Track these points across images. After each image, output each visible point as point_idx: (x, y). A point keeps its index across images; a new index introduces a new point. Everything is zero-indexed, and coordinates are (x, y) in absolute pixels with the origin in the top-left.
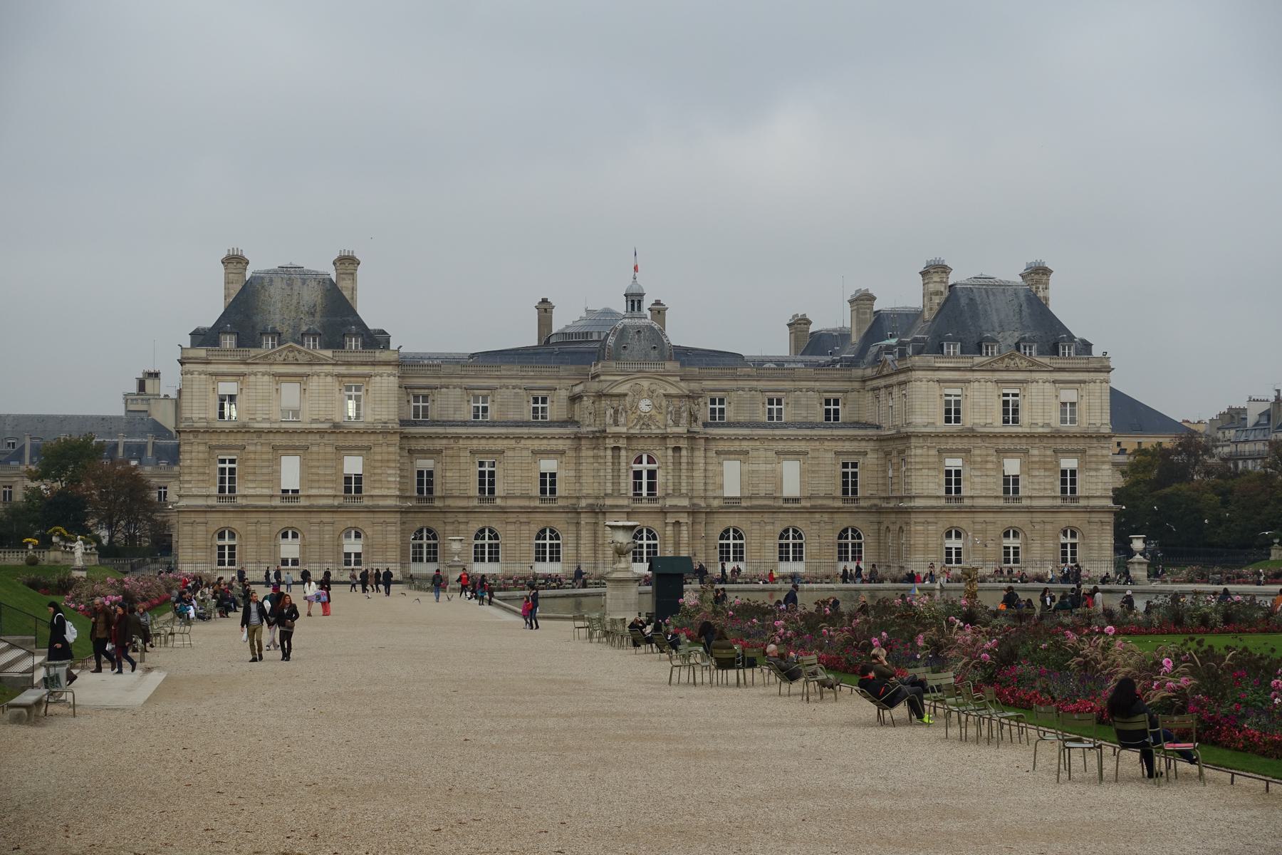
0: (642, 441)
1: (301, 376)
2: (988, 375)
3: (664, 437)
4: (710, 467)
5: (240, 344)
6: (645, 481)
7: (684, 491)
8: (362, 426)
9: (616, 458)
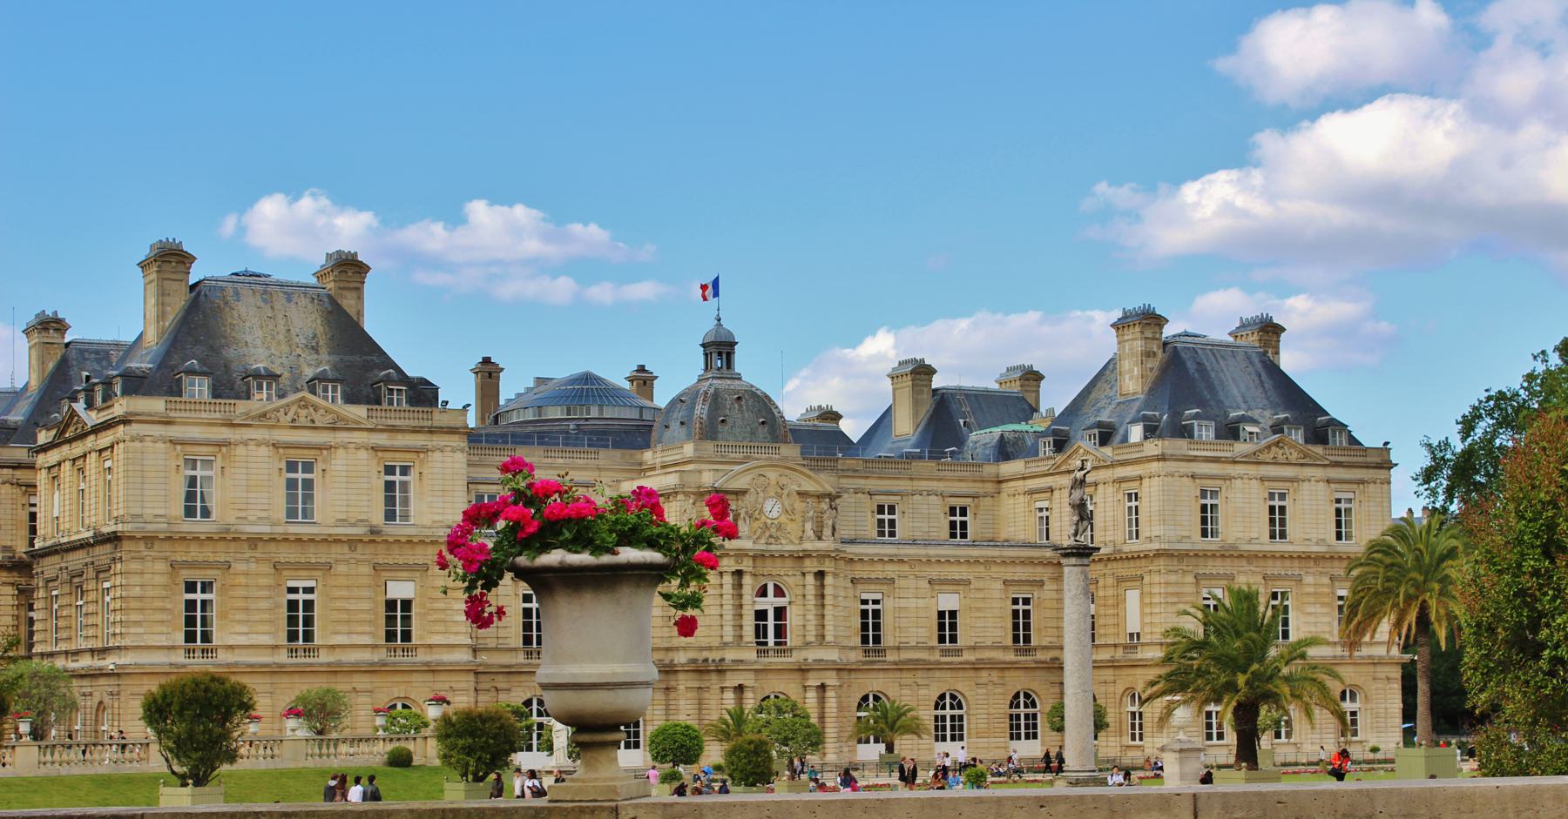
0: (769, 562)
1: (320, 448)
2: (1253, 470)
3: (800, 557)
5: (216, 393)
6: (771, 623)
7: (829, 638)
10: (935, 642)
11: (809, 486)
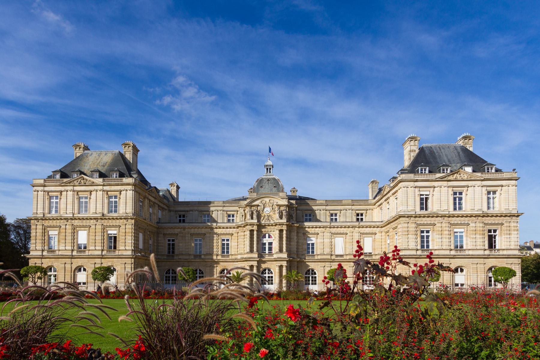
4: (300, 241)
6: (267, 246)
8: (117, 215)
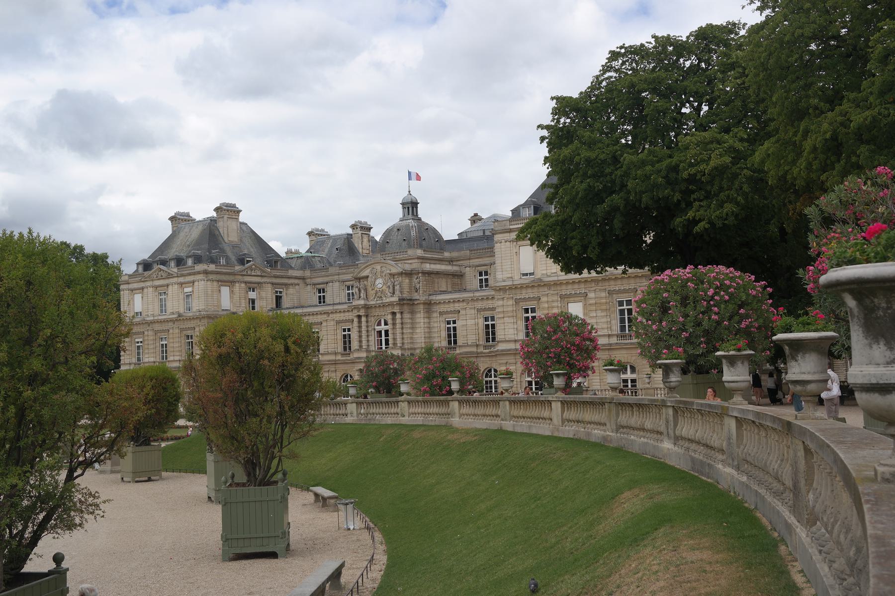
0: (377, 310)
4: (436, 325)
6: (383, 338)
9: (360, 322)
10: (482, 342)
11: (394, 271)
